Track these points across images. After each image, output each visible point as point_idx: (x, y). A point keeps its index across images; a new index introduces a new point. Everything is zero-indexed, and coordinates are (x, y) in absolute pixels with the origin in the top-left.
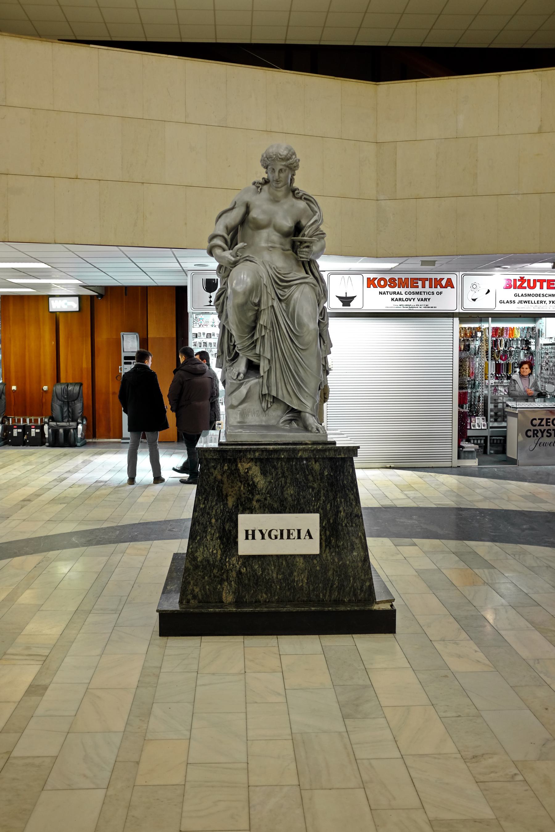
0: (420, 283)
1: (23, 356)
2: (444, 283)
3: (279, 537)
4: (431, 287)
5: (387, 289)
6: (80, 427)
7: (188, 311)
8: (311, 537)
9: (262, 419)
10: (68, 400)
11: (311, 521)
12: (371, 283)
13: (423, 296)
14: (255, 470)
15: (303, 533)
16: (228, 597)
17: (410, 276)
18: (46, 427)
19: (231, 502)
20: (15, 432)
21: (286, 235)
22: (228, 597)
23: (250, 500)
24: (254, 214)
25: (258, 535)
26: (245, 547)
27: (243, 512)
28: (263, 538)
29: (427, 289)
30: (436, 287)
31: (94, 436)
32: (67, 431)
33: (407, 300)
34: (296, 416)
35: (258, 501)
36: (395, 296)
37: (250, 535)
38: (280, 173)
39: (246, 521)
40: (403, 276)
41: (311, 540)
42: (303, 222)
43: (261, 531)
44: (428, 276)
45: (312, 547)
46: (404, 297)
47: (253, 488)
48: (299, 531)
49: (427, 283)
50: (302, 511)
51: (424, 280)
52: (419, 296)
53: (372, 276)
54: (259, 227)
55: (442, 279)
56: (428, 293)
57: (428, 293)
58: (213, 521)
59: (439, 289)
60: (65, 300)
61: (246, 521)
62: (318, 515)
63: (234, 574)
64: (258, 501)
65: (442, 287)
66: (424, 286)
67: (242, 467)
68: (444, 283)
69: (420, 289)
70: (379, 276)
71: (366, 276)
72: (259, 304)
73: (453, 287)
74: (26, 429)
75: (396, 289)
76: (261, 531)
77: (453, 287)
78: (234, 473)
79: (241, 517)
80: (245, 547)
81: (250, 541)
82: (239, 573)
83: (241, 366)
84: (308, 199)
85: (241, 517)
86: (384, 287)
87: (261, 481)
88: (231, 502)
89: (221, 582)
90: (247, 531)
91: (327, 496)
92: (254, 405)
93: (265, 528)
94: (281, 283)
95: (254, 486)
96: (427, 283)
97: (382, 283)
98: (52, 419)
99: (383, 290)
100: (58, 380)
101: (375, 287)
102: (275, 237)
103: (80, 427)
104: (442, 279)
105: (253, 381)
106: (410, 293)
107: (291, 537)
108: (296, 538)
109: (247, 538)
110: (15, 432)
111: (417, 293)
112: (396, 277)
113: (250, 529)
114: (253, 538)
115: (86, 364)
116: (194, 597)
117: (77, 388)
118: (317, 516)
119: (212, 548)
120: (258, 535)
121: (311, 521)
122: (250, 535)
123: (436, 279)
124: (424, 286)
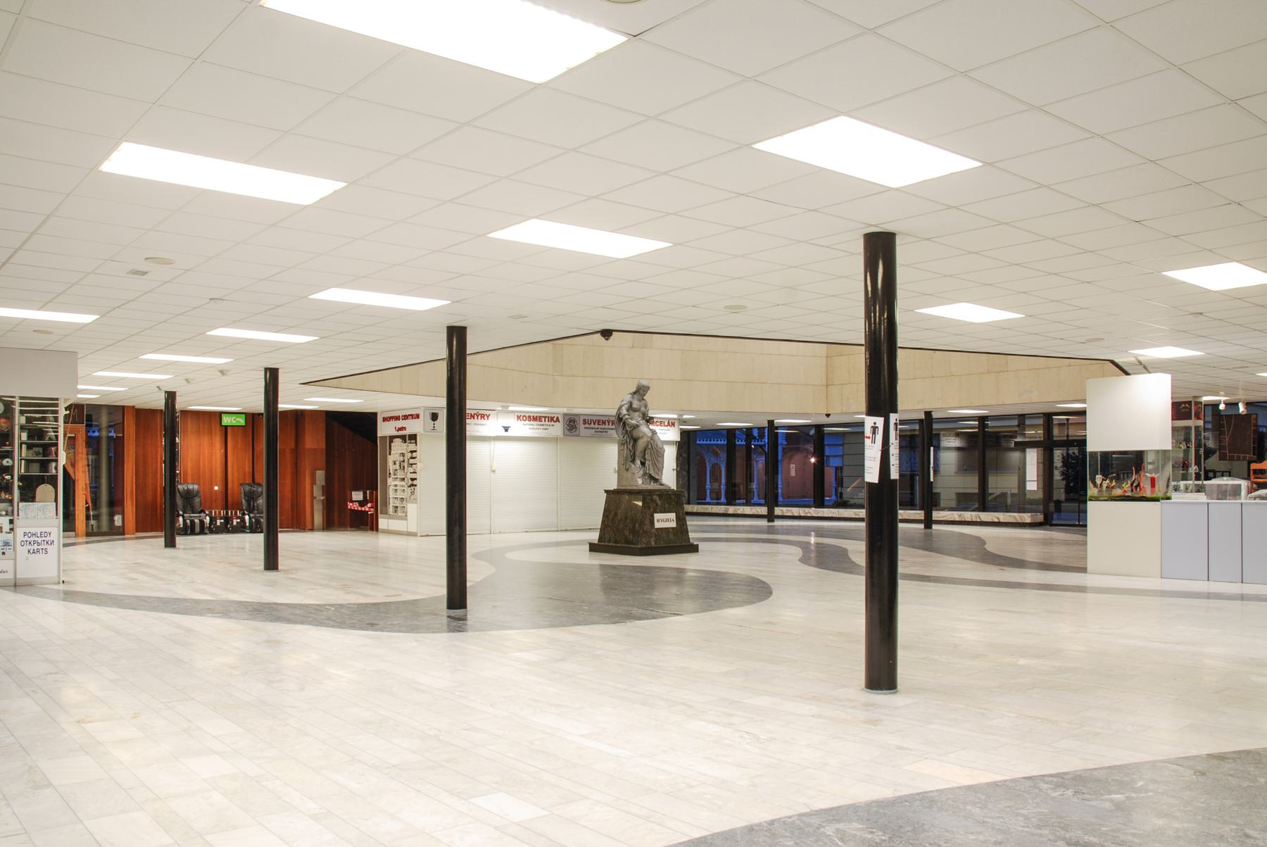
11: (673, 516)
20: (218, 522)
24: (634, 406)
26: (657, 525)
34: (656, 480)
38: (641, 391)
45: (674, 525)
54: (636, 410)
60: (234, 417)
61: (657, 516)
67: (654, 497)
74: (227, 520)
78: (652, 500)
80: (657, 525)
83: (638, 462)
110: (218, 522)
115: (248, 468)
121: (673, 516)
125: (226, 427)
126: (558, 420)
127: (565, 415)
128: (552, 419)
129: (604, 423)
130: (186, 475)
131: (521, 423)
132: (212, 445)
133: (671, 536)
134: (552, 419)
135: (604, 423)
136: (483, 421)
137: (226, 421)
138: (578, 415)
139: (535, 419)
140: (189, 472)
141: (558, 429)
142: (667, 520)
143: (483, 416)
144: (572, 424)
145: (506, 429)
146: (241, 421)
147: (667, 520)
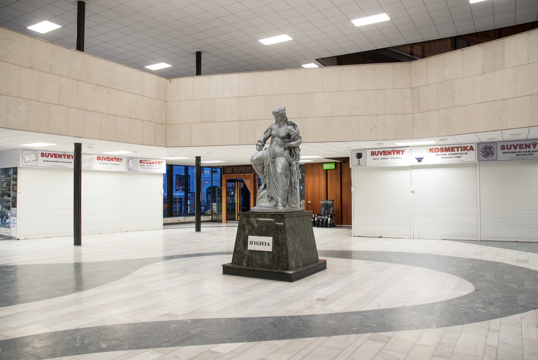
0: (456, 149)
1: (313, 189)
2: (468, 148)
4: (461, 150)
5: (439, 153)
6: (329, 219)
7: (350, 167)
9: (268, 204)
10: (327, 207)
11: (269, 240)
12: (431, 150)
13: (458, 155)
15: (267, 244)
16: (245, 264)
17: (450, 146)
18: (316, 219)
19: (247, 231)
21: (283, 138)
22: (245, 264)
23: (252, 231)
25: (253, 243)
26: (250, 247)
29: (460, 152)
30: (464, 150)
31: (342, 224)
32: (323, 221)
33: (449, 157)
36: (443, 156)
37: (251, 243)
39: (251, 238)
40: (447, 147)
42: (291, 134)
44: (460, 146)
45: (269, 249)
46: (448, 156)
47: (253, 227)
49: (460, 149)
50: (267, 236)
51: (458, 148)
52: (456, 156)
53: (431, 147)
54: (273, 137)
55: (467, 147)
56: (460, 154)
57: (460, 154)
59: (466, 151)
60: (329, 164)
61: (251, 238)
62: (271, 238)
63: (246, 256)
65: (467, 150)
66: (458, 150)
68: (468, 148)
69: (456, 152)
70: (435, 147)
71: (429, 147)
72: (263, 164)
73: (473, 150)
75: (444, 153)
77: (473, 150)
78: (248, 222)
79: (249, 237)
80: (250, 247)
82: (248, 256)
84: (294, 125)
85: (249, 237)
86: (438, 152)
88: (247, 231)
89: (243, 259)
91: (275, 231)
92: (266, 199)
93: (256, 241)
94: (274, 156)
95: (254, 226)
96: (460, 149)
97: (437, 150)
98: (319, 215)
99: (437, 154)
100: (327, 199)
101: (433, 152)
102: (279, 140)
103: (329, 219)
104: (467, 147)
105: (265, 191)
106: (451, 154)
111: (455, 154)
112: (444, 147)
115: (338, 192)
116: (235, 263)
117: (331, 202)
118: (271, 238)
119: (241, 247)
120: (253, 243)
121: (269, 240)
122: (251, 243)
123: (464, 147)
124: (458, 150)
125: (327, 170)
126: (471, 148)
127: (479, 144)
128: (465, 148)
129: (528, 146)
130: (307, 195)
131: (433, 154)
132: (320, 181)
133: (266, 261)
134: (465, 148)
135: (528, 146)
136: (398, 156)
137: (326, 167)
138: (496, 143)
139: (447, 150)
140: (309, 194)
141: (471, 156)
142: (261, 244)
143: (398, 152)
144: (487, 151)
145: (419, 160)
146: (333, 166)
147: (261, 244)
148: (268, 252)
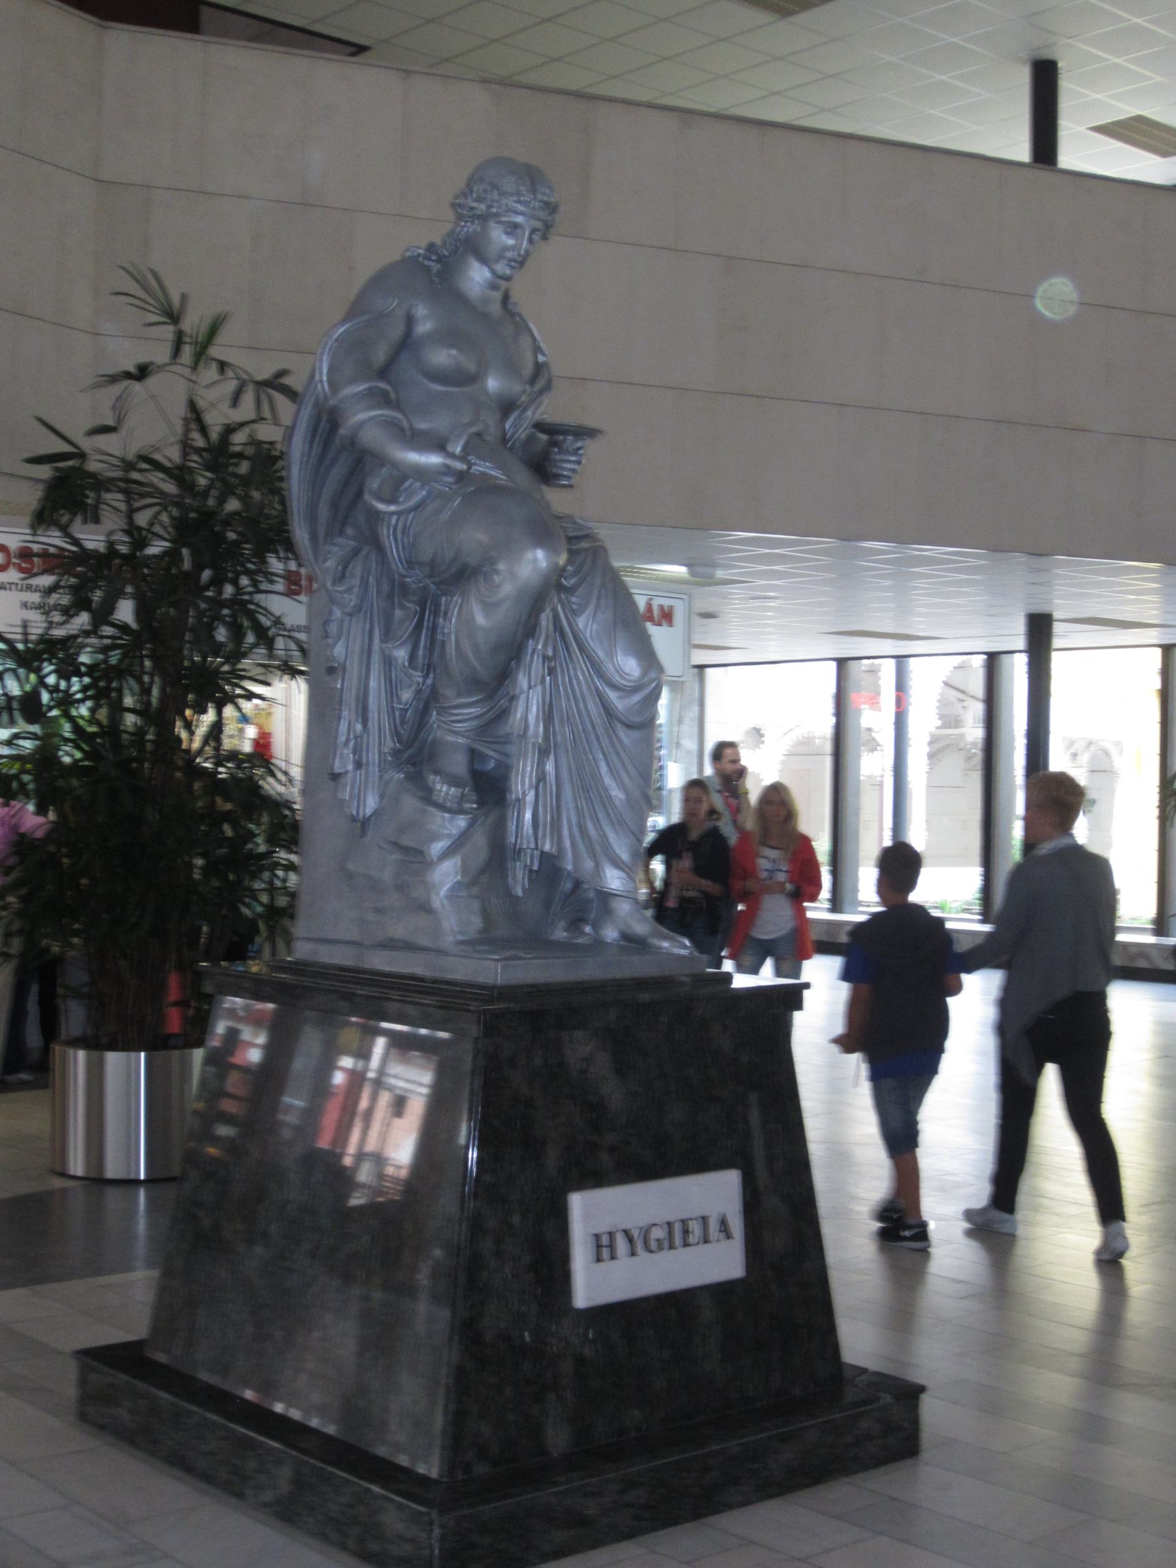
3: (666, 1244)
8: (729, 1236)
14: (602, 1065)
15: (713, 1226)
19: (552, 1158)
25: (621, 1245)
26: (591, 1284)
27: (580, 1187)
28: (633, 1254)
35: (612, 1149)
39: (588, 1211)
41: (730, 1241)
43: (626, 1233)
48: (704, 1220)
58: (516, 1219)
61: (588, 1211)
64: (612, 1149)
76: (626, 1233)
79: (576, 1201)
80: (591, 1284)
81: (607, 1265)
85: (576, 1201)
87: (614, 1094)
88: (552, 1158)
90: (597, 1237)
93: (634, 1223)
107: (692, 1239)
108: (702, 1240)
109: (599, 1260)
113: (602, 1228)
114: (613, 1257)
120: (621, 1245)
122: (603, 1248)
142: (679, 1234)
147: (679, 1234)
148: (721, 1291)
